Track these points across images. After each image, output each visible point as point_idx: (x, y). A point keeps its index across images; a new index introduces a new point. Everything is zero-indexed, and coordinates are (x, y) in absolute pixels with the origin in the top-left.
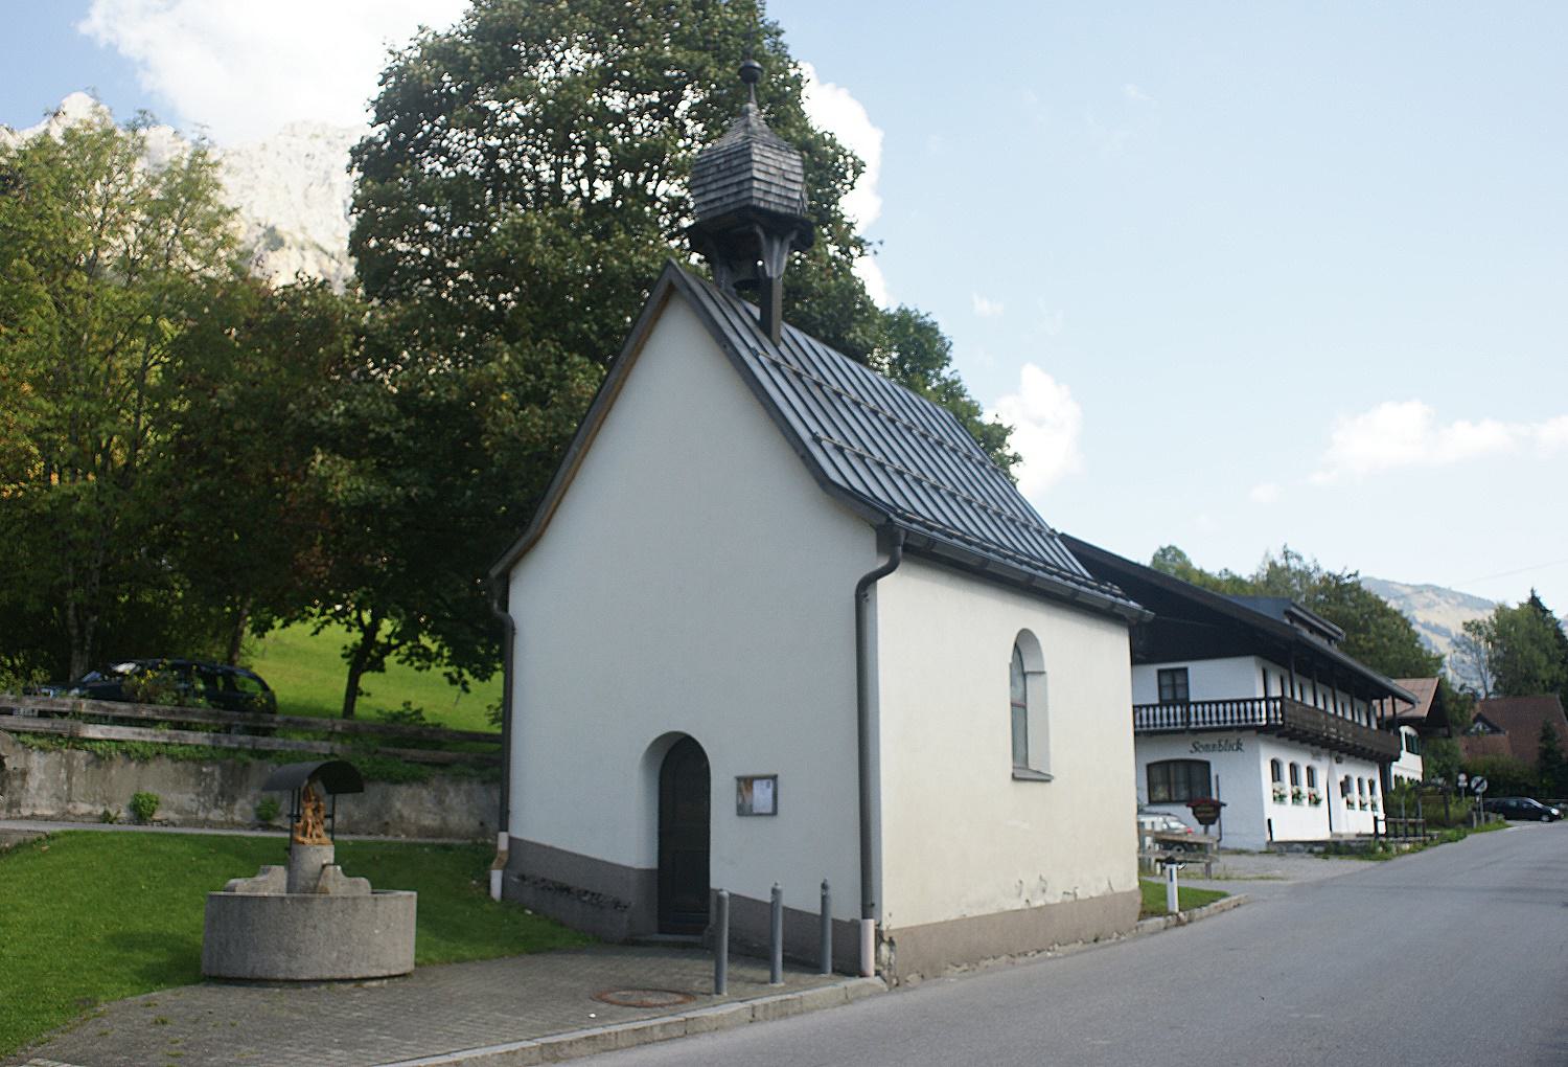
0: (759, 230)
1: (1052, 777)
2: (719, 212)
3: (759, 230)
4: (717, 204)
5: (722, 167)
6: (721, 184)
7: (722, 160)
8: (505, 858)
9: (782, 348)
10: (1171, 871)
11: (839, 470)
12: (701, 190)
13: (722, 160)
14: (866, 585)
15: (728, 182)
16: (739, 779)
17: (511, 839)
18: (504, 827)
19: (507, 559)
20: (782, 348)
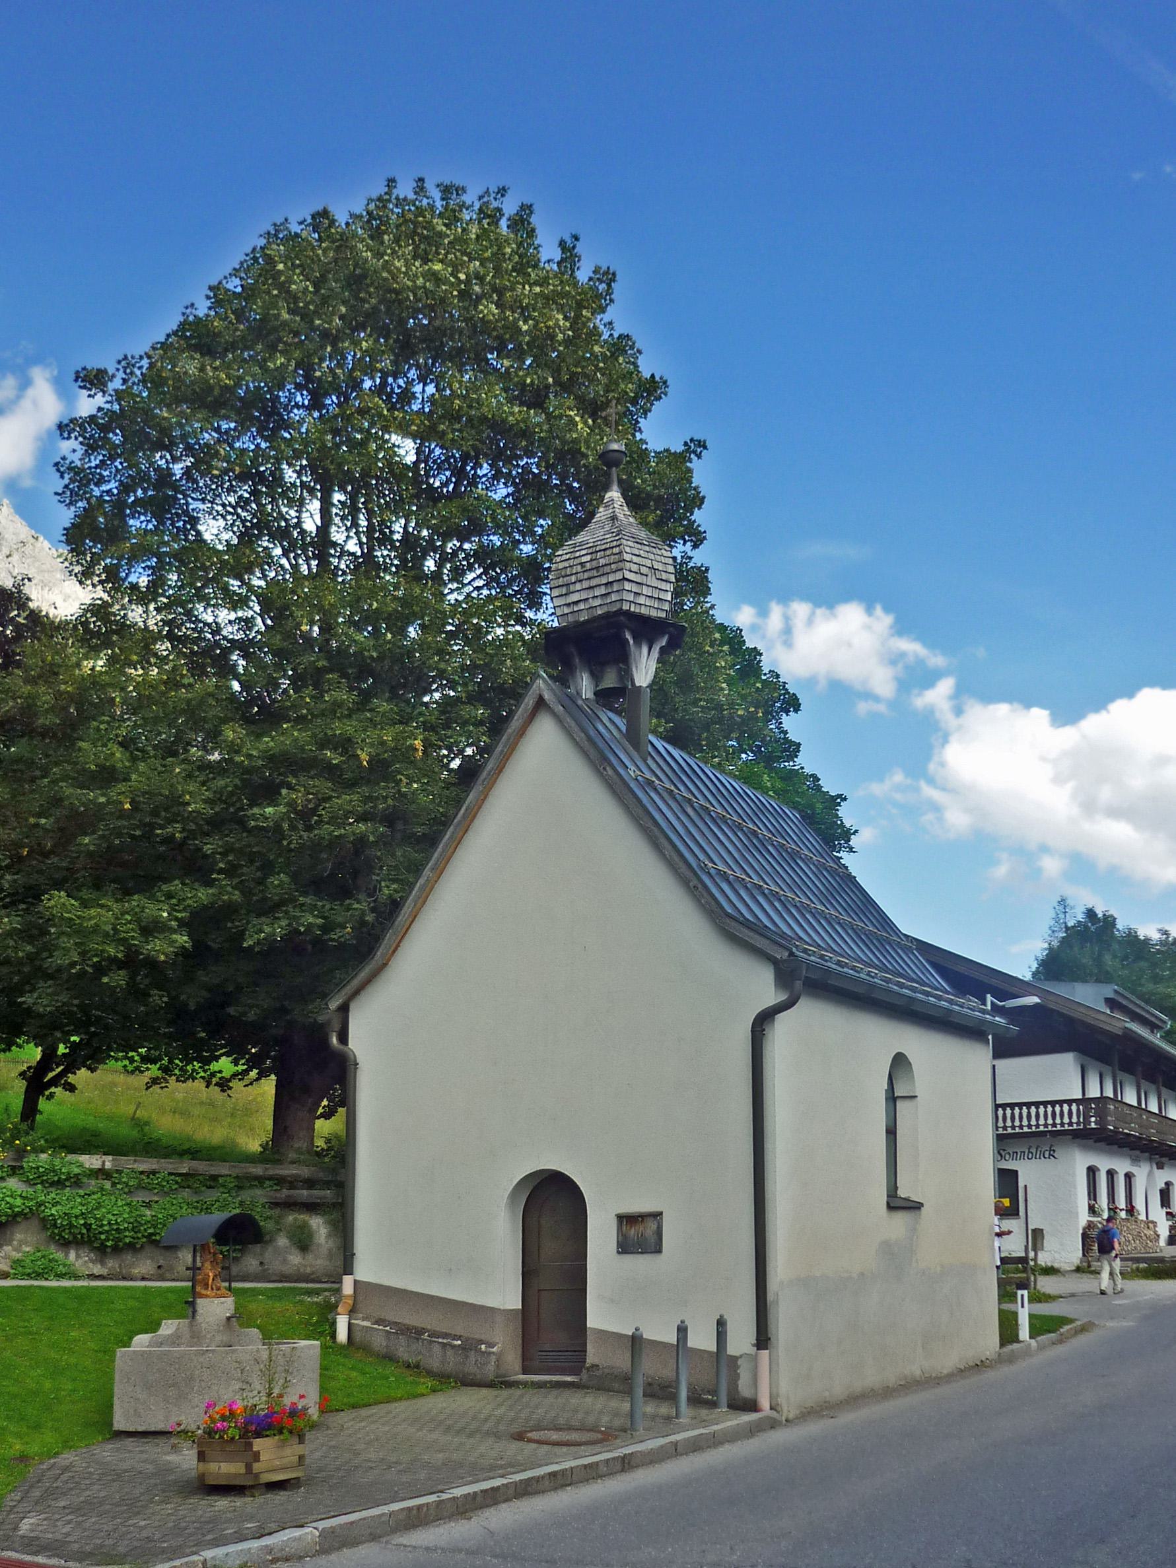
0: (628, 636)
1: (922, 1205)
2: (583, 617)
3: (628, 636)
4: (582, 606)
5: (588, 566)
6: (585, 584)
7: (588, 558)
8: (351, 1302)
9: (650, 761)
10: (1022, 1296)
11: (730, 899)
12: (564, 590)
13: (588, 558)
14: (764, 1020)
15: (594, 582)
16: (621, 1218)
17: (356, 1282)
18: (348, 1270)
19: (349, 989)
20: (650, 761)
